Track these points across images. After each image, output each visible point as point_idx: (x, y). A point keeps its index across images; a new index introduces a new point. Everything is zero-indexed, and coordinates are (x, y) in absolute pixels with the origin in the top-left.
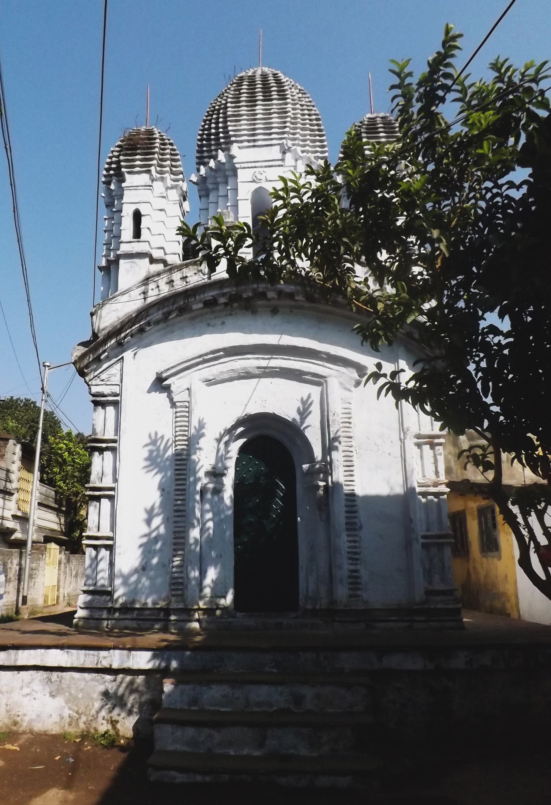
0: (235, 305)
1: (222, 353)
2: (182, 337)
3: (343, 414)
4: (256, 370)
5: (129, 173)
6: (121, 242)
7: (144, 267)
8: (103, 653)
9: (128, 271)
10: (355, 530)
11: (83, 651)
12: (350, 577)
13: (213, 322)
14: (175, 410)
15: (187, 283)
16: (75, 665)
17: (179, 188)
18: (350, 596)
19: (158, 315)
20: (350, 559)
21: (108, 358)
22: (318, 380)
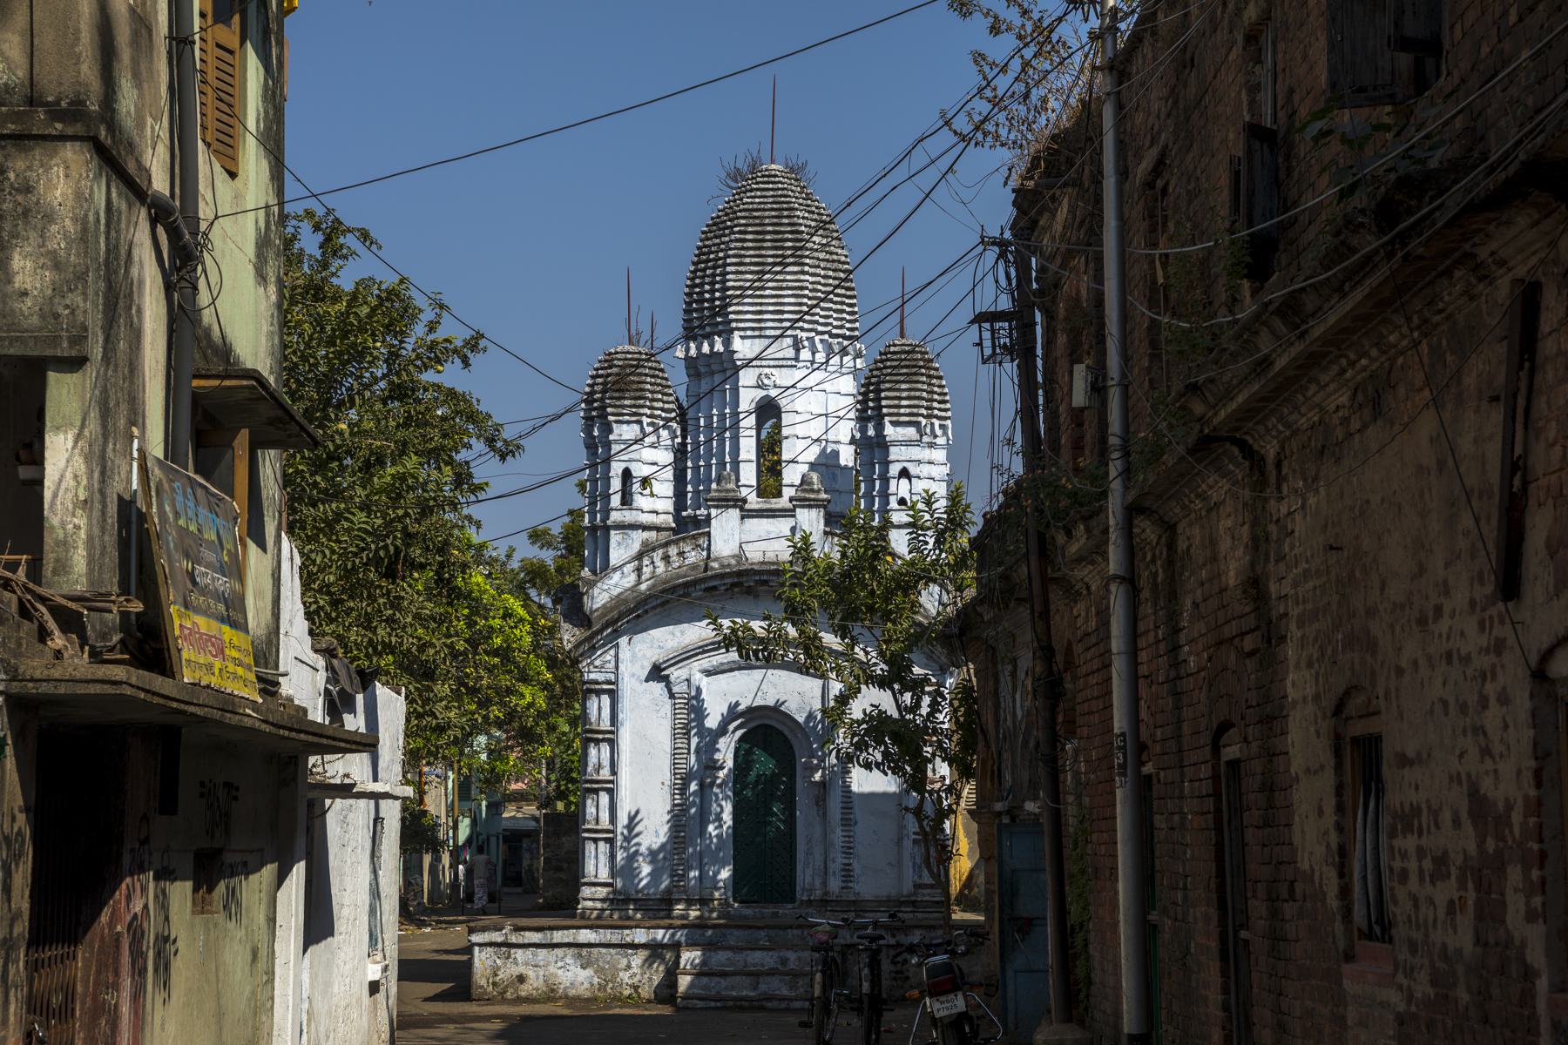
2: (681, 622)
21: (603, 645)
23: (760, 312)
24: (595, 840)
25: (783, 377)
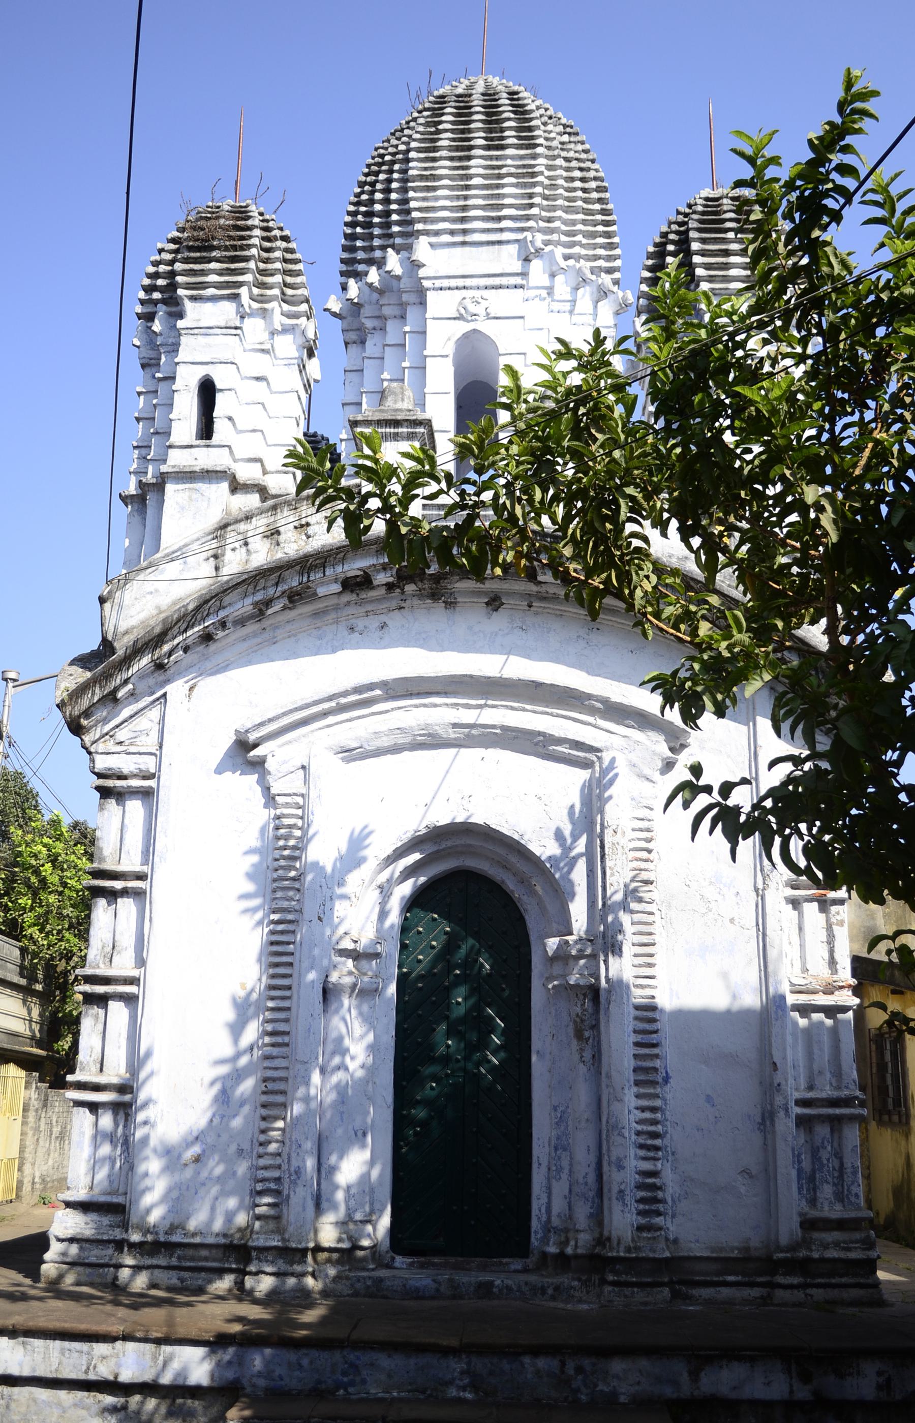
0: (410, 588)
1: (378, 692)
2: (295, 655)
3: (633, 830)
4: (451, 730)
5: (193, 298)
6: (170, 447)
7: (217, 501)
8: (101, 1348)
9: (183, 508)
10: (654, 1083)
11: (58, 1343)
12: (640, 1187)
13: (360, 624)
14: (273, 812)
15: (308, 537)
16: (38, 1373)
17: (298, 332)
18: (640, 1228)
19: (242, 606)
20: (642, 1146)
21: (133, 696)
22: (580, 755)
23: (464, 208)
24: (93, 1107)
25: (503, 302)
